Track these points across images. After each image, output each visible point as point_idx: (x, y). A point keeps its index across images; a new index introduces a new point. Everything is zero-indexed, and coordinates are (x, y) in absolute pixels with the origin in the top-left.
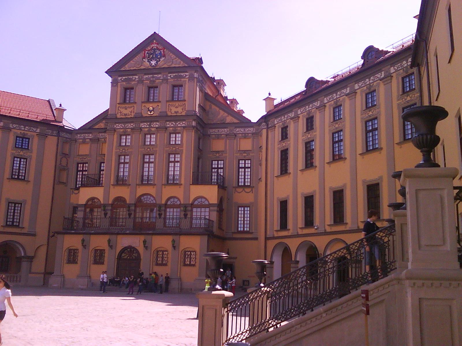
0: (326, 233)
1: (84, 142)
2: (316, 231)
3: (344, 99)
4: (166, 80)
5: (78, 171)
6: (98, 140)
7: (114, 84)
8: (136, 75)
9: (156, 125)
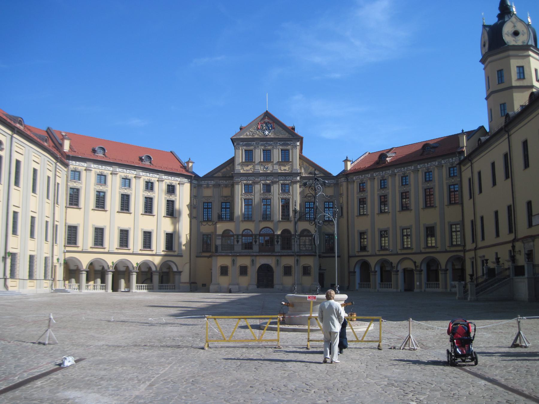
0: (397, 254)
1: (208, 186)
2: (390, 253)
3: (410, 173)
5: (204, 208)
6: (219, 185)
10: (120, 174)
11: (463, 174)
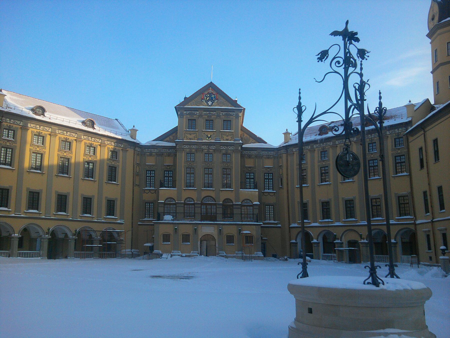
4: (219, 116)
7: (180, 116)
8: (198, 111)
9: (213, 147)
10: (59, 135)
11: (411, 144)
